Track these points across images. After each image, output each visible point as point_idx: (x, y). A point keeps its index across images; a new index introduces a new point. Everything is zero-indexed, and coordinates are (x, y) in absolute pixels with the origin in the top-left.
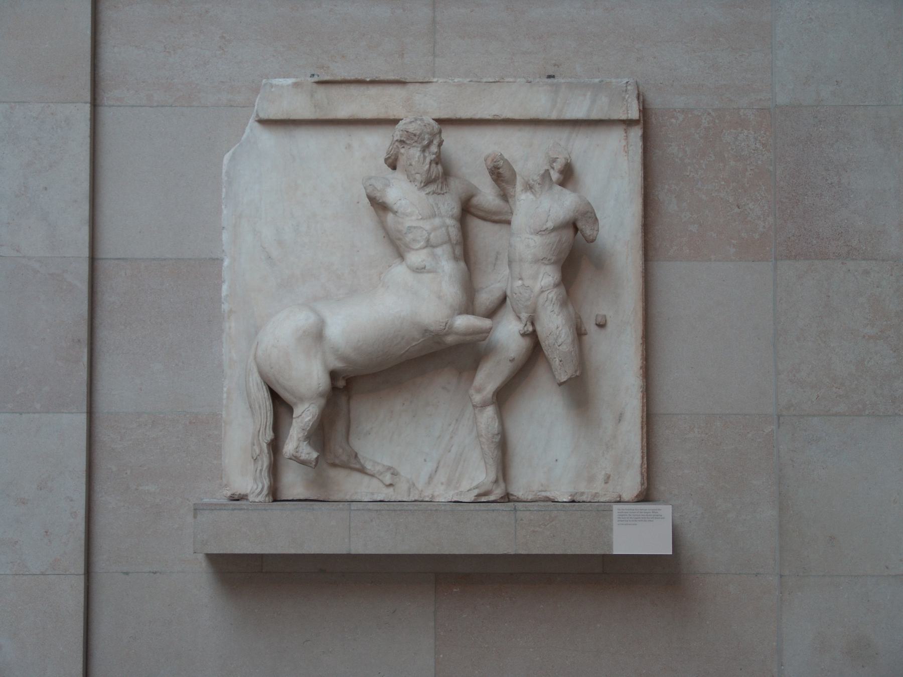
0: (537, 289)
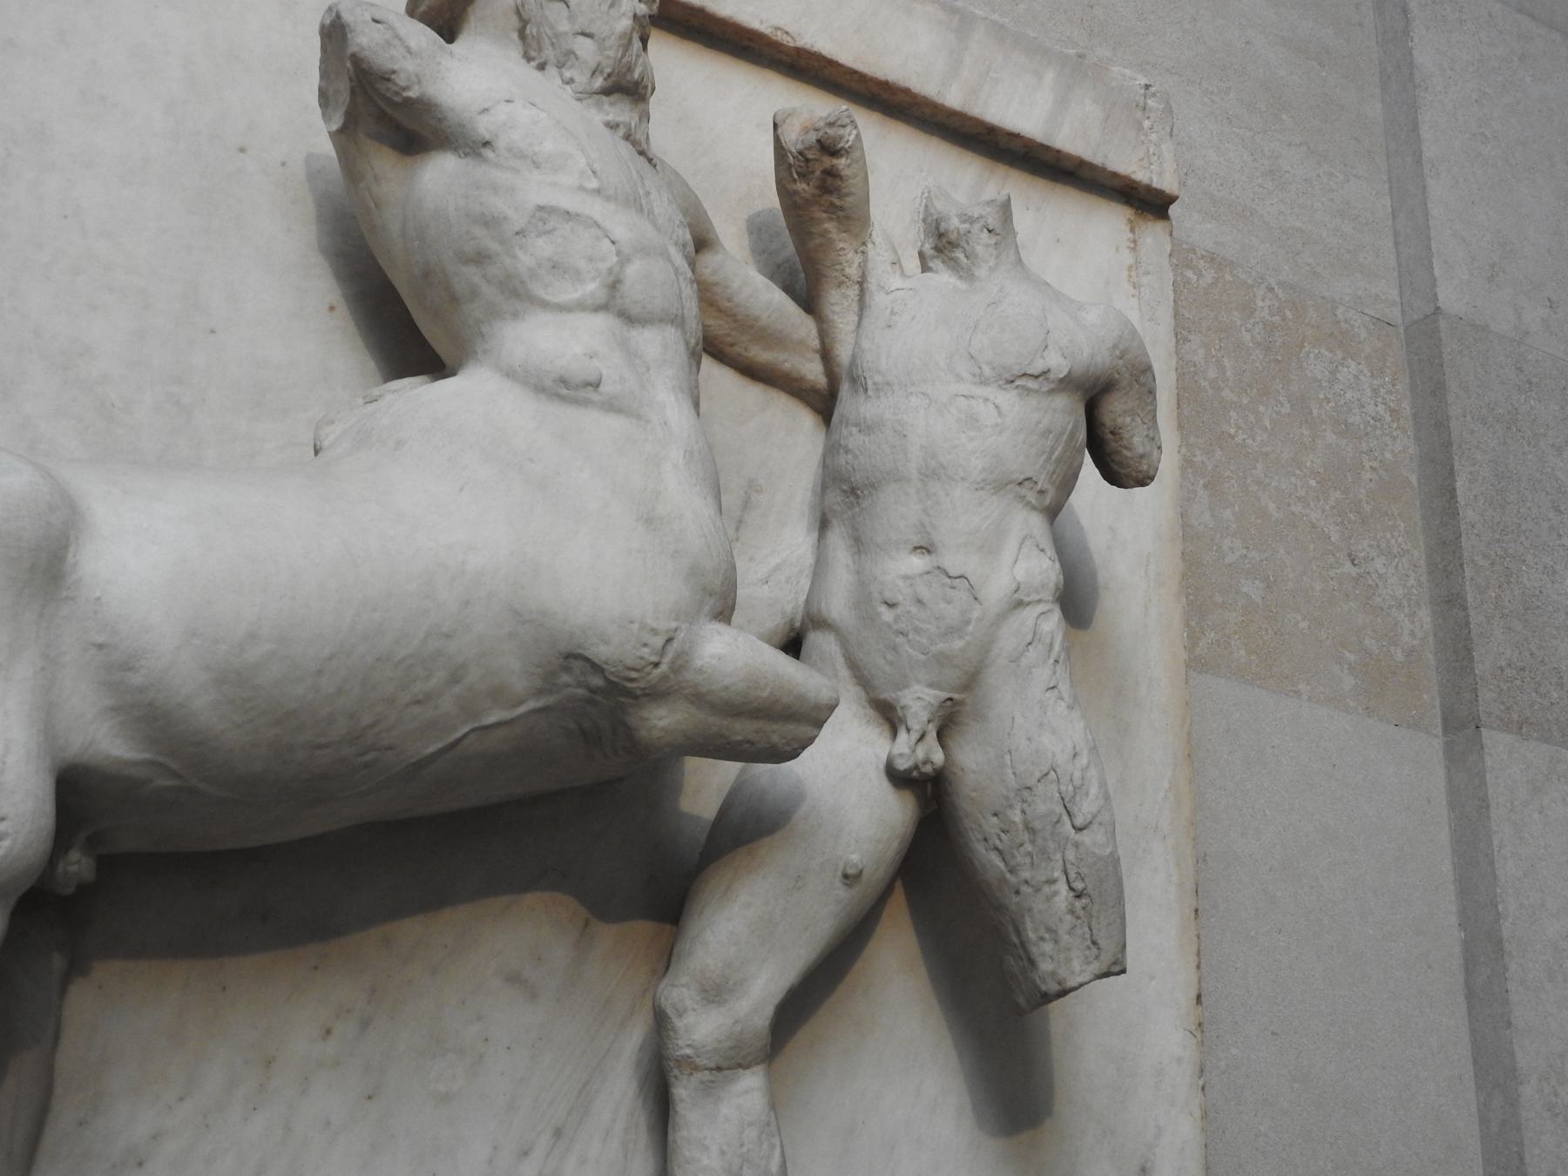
0: (997, 588)
